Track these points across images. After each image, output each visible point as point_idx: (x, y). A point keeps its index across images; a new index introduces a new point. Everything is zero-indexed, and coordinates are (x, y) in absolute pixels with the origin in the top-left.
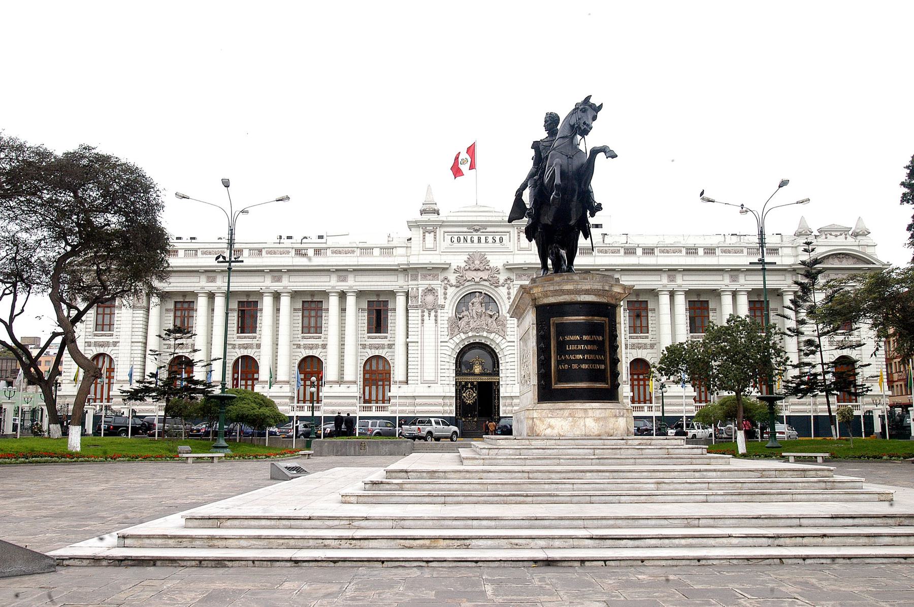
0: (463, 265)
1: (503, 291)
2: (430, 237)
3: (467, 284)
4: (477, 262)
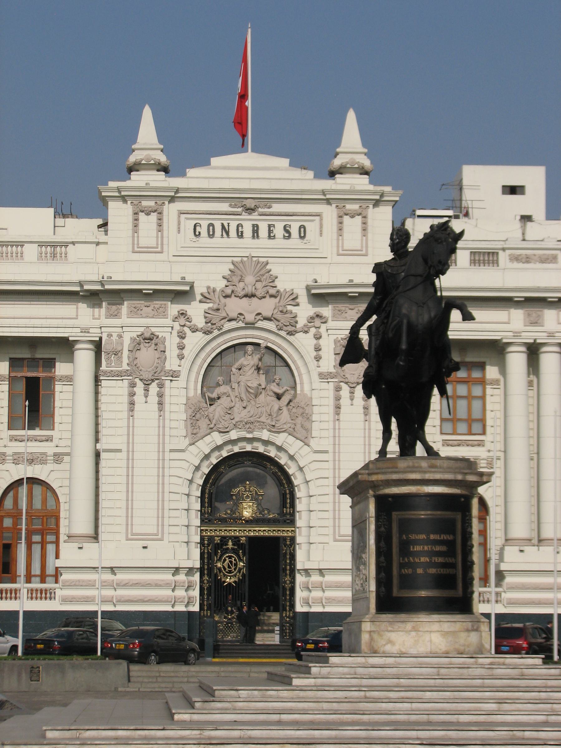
0: (220, 284)
1: (305, 342)
2: (148, 223)
3: (228, 326)
4: (250, 279)
